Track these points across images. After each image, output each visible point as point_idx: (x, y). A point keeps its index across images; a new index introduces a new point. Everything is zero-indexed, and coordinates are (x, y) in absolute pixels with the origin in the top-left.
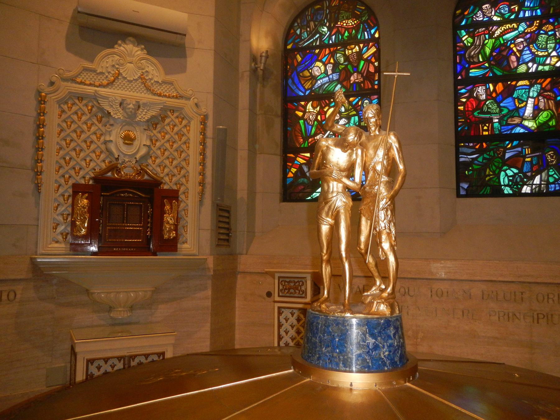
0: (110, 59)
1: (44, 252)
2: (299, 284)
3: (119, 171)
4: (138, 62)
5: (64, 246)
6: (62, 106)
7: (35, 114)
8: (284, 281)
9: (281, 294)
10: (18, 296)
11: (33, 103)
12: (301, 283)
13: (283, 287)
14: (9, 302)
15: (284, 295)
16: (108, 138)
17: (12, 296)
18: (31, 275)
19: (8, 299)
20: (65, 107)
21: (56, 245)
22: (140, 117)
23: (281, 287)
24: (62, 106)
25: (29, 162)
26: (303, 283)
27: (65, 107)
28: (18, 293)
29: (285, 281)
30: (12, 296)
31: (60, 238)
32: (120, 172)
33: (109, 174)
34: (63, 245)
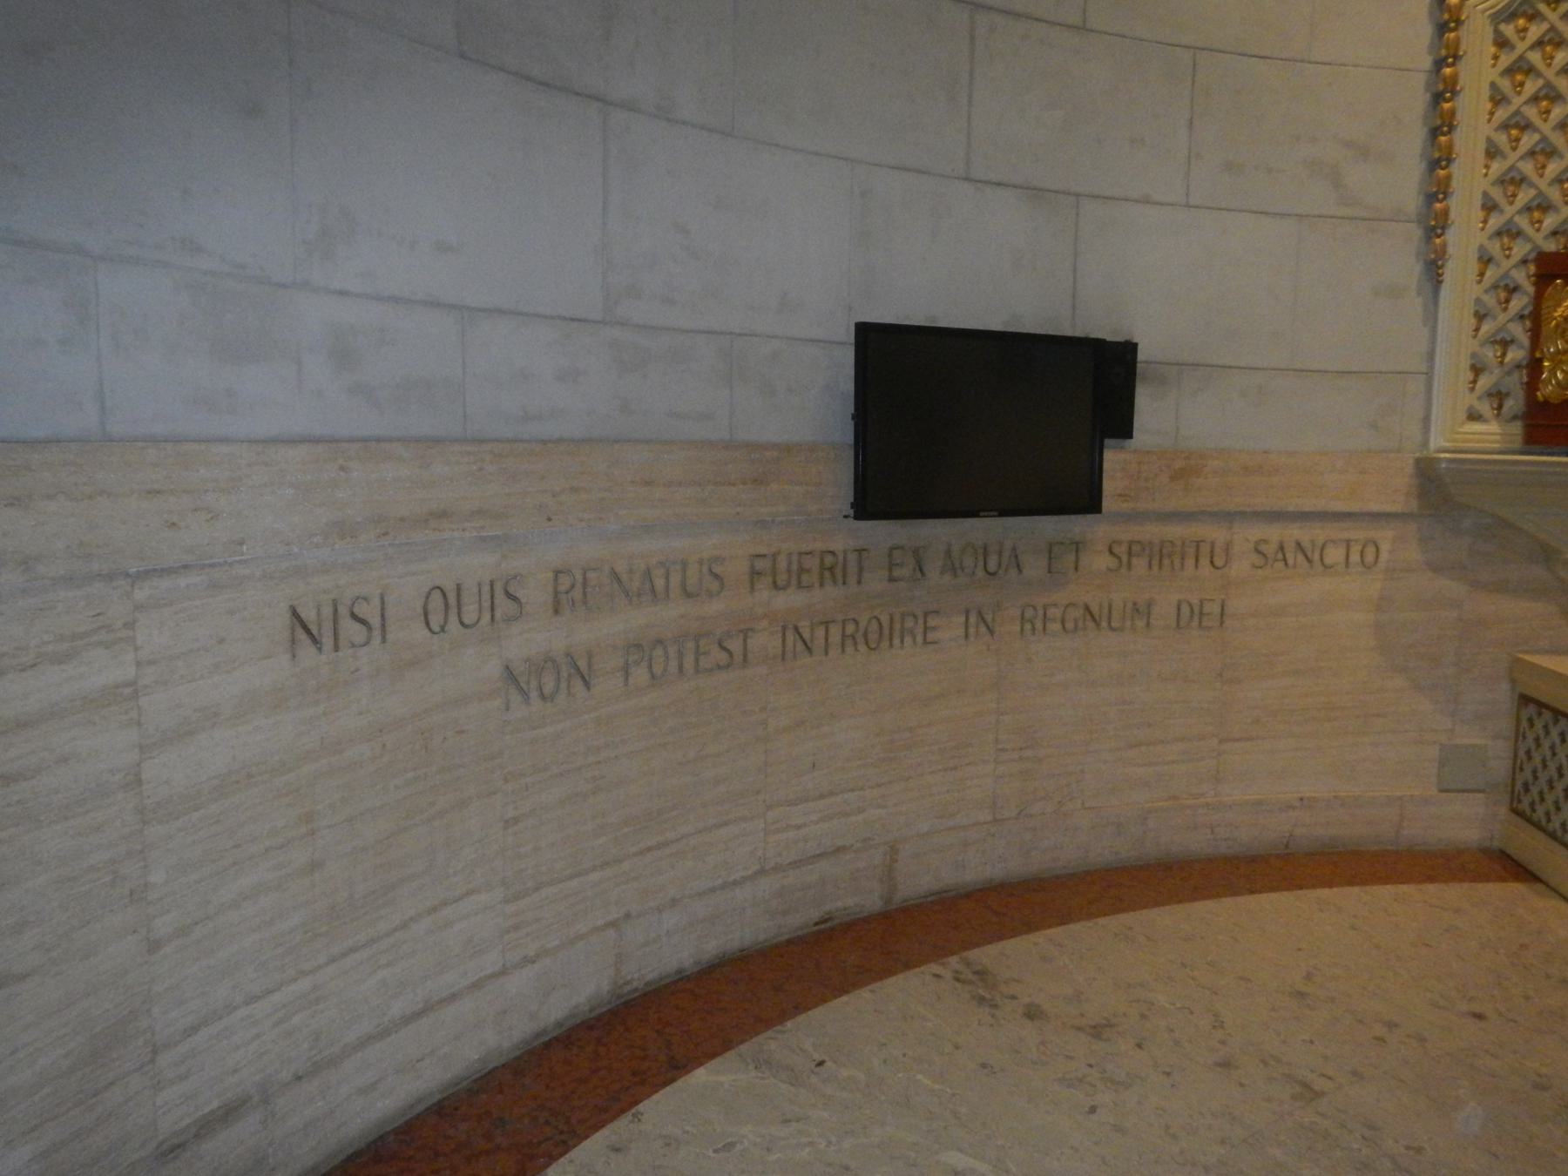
1: (1447, 444)
5: (1498, 431)
6: (1502, 27)
7: (1427, 62)
10: (1384, 556)
11: (1426, 31)
17: (1370, 557)
18: (1414, 505)
20: (1508, 30)
21: (1477, 427)
24: (1502, 27)
25: (1411, 200)
27: (1508, 30)
28: (1385, 547)
30: (1370, 557)
31: (1485, 408)
34: (1493, 427)
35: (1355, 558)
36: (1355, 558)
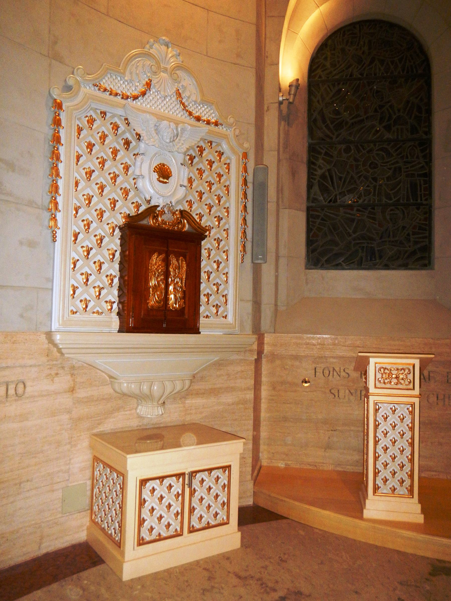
0: (140, 64)
2: (404, 371)
3: (155, 217)
4: (173, 72)
8: (383, 368)
9: (378, 385)
10: (28, 389)
12: (407, 371)
13: (382, 377)
14: (17, 398)
15: (383, 386)
16: (137, 173)
19: (16, 393)
22: (178, 146)
23: (379, 376)
26: (409, 370)
29: (385, 369)
32: (157, 220)
33: (144, 222)
35: (11, 391)
36: (11, 391)
